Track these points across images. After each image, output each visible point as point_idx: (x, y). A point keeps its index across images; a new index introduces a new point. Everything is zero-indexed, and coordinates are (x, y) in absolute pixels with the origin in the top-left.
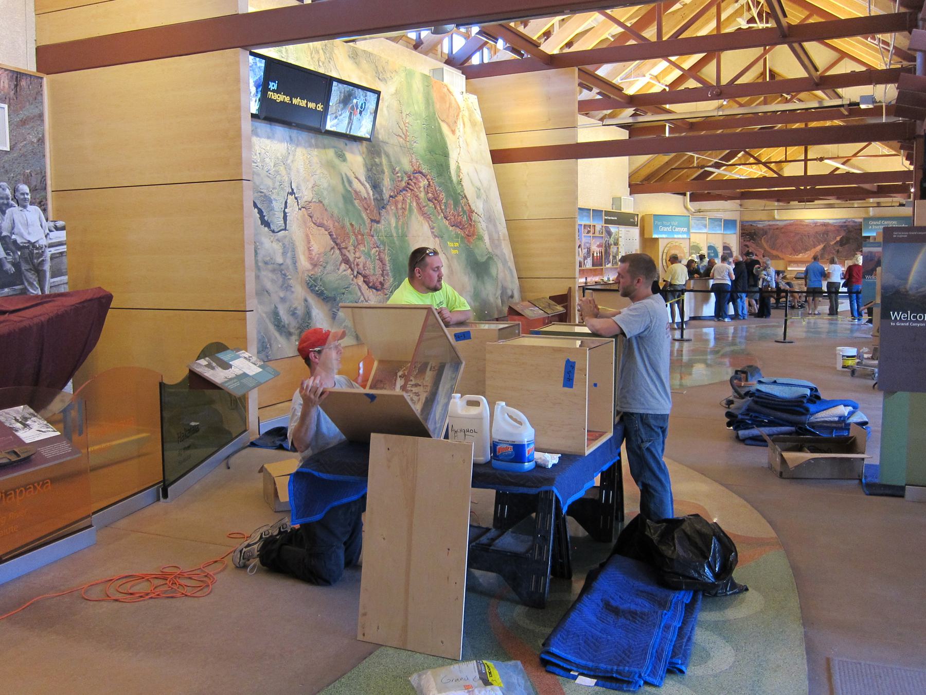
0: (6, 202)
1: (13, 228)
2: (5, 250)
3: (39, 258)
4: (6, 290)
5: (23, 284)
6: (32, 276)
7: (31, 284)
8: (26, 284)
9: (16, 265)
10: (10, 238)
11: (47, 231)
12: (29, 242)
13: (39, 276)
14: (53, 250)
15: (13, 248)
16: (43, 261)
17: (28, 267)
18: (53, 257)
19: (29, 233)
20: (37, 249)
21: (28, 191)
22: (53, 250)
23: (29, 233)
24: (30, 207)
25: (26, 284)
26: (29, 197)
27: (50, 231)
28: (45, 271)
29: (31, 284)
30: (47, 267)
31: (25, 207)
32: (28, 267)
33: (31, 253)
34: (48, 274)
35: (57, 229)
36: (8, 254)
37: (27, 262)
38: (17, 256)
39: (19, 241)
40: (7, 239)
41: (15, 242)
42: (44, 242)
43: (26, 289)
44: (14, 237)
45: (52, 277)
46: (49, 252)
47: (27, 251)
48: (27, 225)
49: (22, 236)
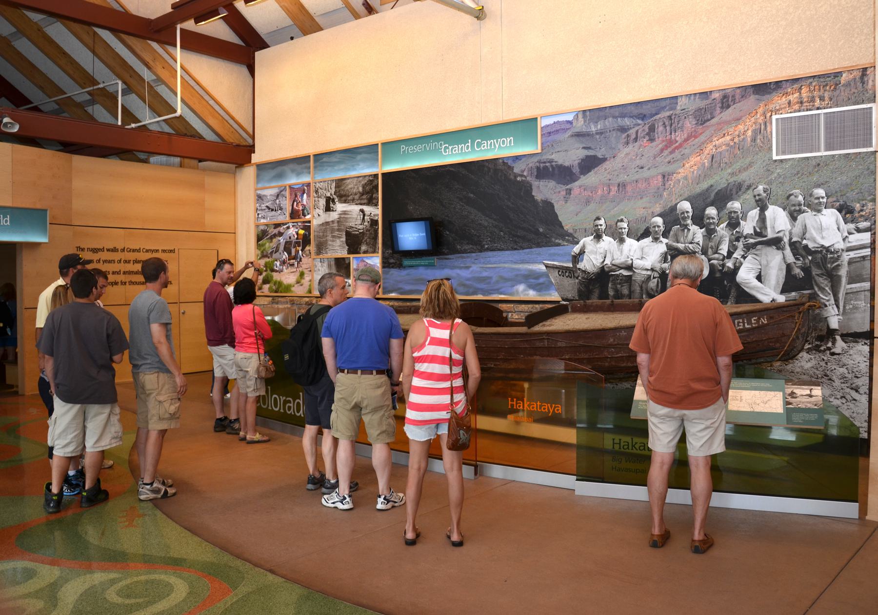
0: (797, 208)
1: (804, 234)
2: (794, 255)
3: (833, 262)
4: (793, 294)
5: (813, 288)
6: (824, 282)
7: (822, 290)
8: (816, 289)
9: (806, 270)
10: (801, 243)
11: (846, 234)
12: (822, 246)
13: (831, 281)
14: (852, 254)
15: (804, 253)
16: (839, 265)
17: (819, 272)
18: (851, 262)
19: (823, 238)
20: (832, 253)
21: (824, 195)
22: (852, 254)
23: (823, 238)
24: (825, 211)
25: (816, 289)
26: (825, 200)
27: (850, 233)
28: (839, 277)
29: (822, 290)
30: (843, 272)
31: (819, 211)
32: (819, 272)
33: (824, 258)
34: (844, 280)
35: (859, 230)
36: (797, 259)
37: (818, 266)
38: (807, 261)
39: (811, 245)
40: (798, 245)
41: (806, 246)
42: (841, 245)
43: (815, 294)
44: (805, 242)
45: (849, 283)
46: (846, 257)
47: (820, 255)
48: (821, 229)
49: (815, 242)
